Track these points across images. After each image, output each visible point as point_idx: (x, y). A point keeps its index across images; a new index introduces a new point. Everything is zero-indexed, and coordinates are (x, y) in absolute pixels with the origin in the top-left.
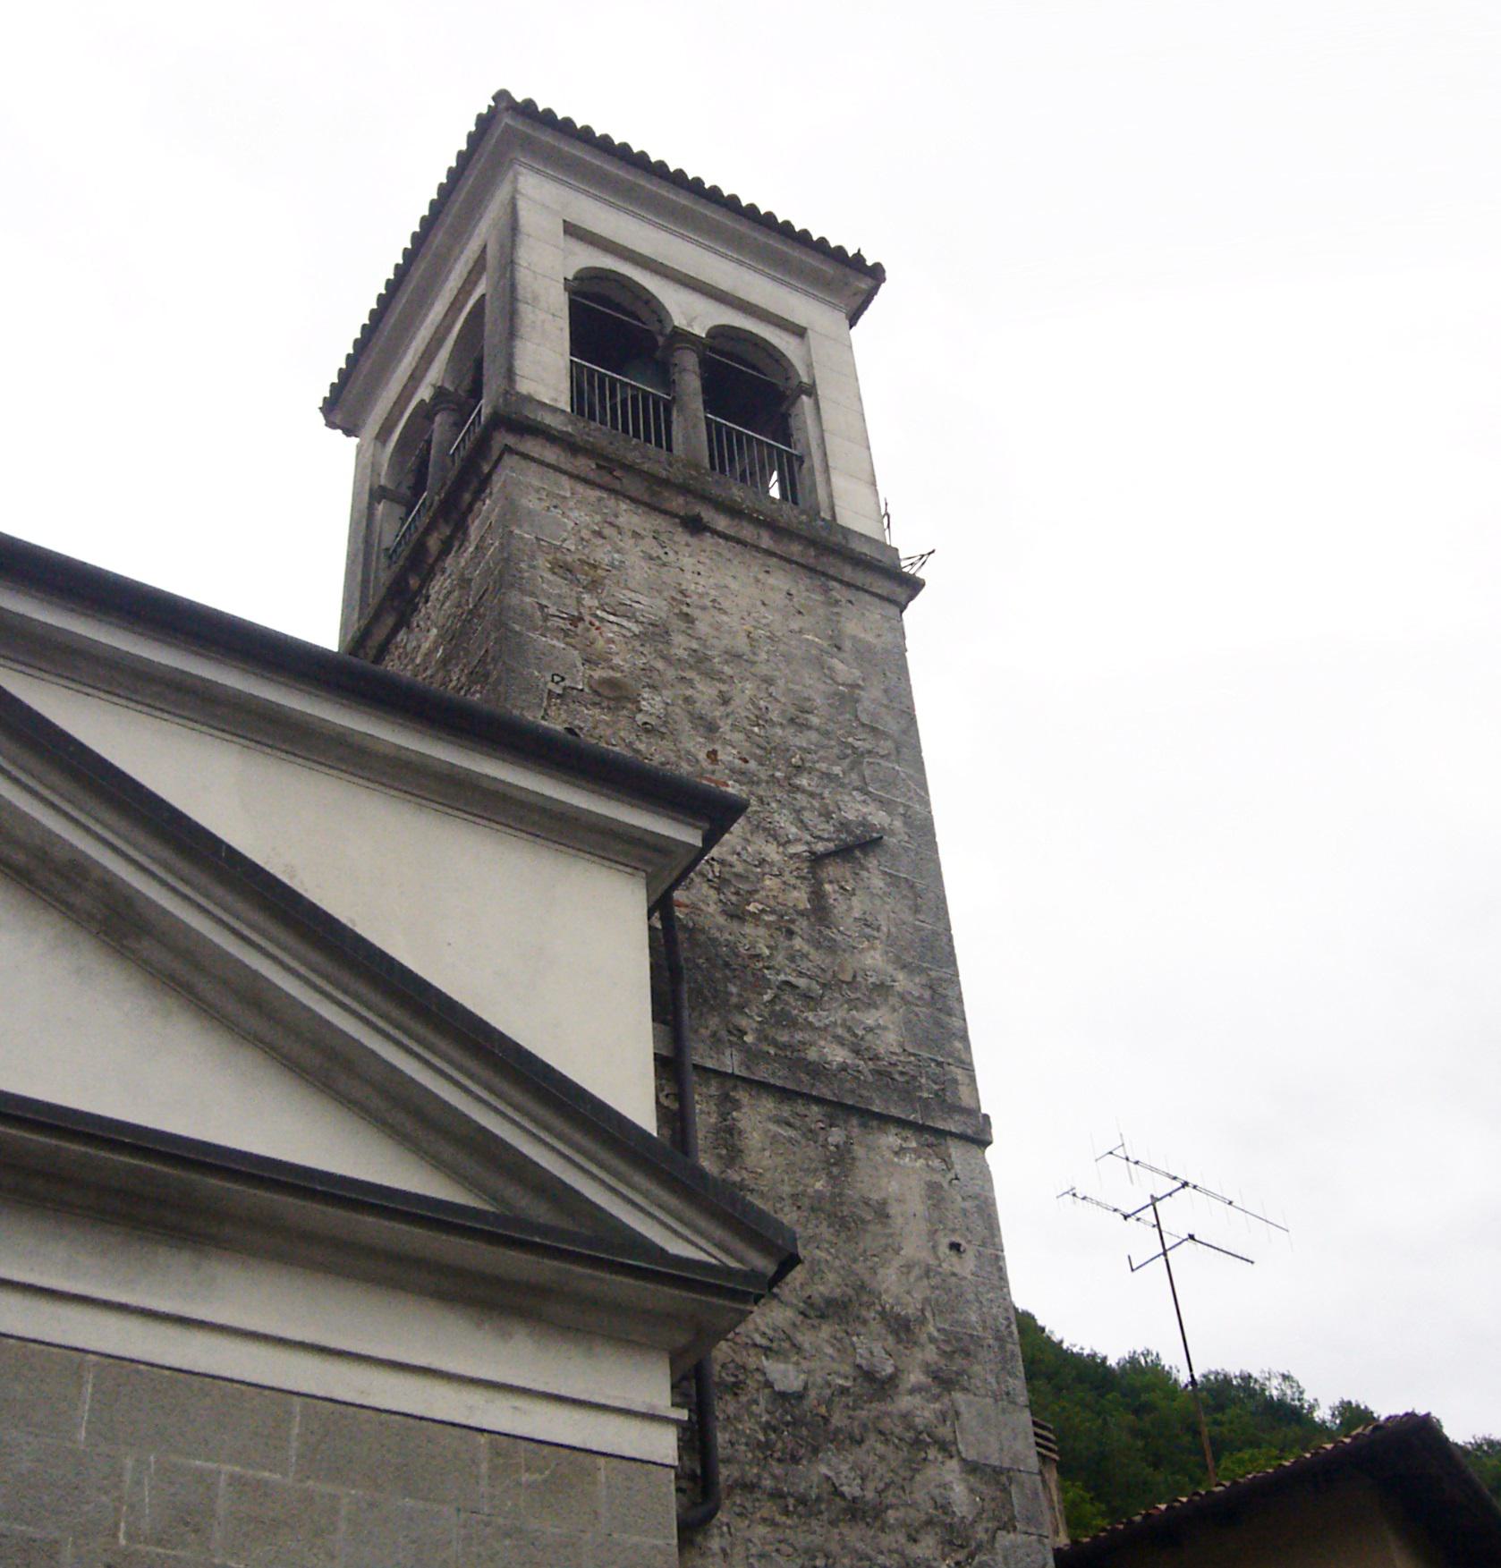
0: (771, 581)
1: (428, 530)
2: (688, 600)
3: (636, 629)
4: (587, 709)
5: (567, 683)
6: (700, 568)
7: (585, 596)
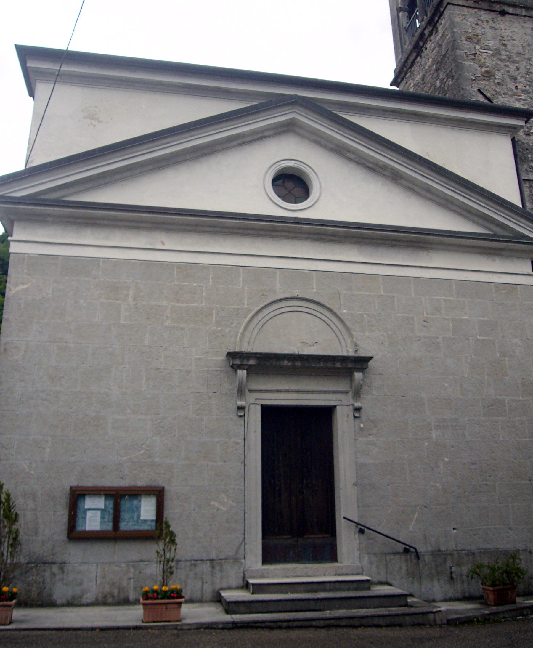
0: (527, 25)
1: (424, 29)
2: (504, 39)
3: (491, 52)
4: (482, 82)
5: (476, 75)
6: (506, 27)
7: (476, 46)
